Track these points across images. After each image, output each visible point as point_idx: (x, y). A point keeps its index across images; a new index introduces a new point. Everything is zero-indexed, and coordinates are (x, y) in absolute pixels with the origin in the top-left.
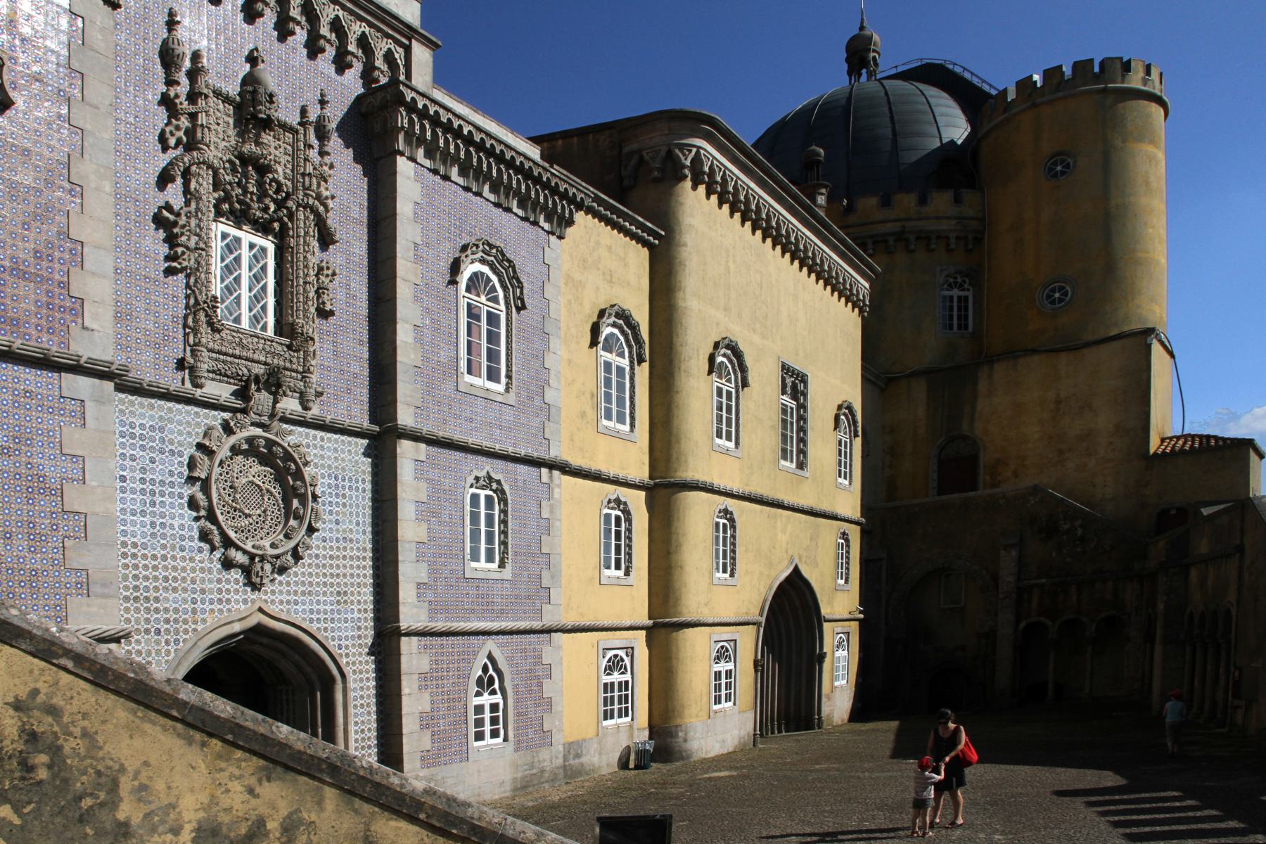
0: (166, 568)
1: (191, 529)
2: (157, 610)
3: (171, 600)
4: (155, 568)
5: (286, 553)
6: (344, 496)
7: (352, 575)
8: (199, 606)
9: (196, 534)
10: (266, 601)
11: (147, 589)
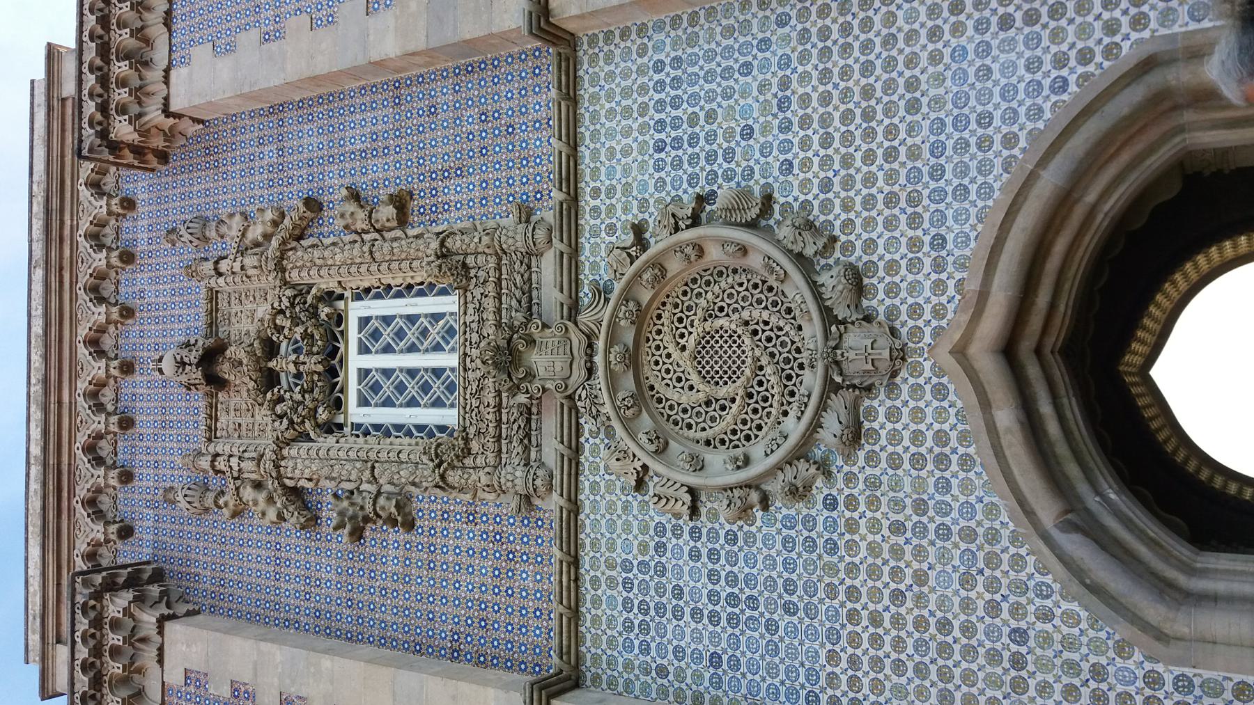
0: (875, 594)
1: (790, 523)
2: (968, 630)
3: (944, 590)
4: (876, 620)
10: (937, 332)
11: (921, 645)
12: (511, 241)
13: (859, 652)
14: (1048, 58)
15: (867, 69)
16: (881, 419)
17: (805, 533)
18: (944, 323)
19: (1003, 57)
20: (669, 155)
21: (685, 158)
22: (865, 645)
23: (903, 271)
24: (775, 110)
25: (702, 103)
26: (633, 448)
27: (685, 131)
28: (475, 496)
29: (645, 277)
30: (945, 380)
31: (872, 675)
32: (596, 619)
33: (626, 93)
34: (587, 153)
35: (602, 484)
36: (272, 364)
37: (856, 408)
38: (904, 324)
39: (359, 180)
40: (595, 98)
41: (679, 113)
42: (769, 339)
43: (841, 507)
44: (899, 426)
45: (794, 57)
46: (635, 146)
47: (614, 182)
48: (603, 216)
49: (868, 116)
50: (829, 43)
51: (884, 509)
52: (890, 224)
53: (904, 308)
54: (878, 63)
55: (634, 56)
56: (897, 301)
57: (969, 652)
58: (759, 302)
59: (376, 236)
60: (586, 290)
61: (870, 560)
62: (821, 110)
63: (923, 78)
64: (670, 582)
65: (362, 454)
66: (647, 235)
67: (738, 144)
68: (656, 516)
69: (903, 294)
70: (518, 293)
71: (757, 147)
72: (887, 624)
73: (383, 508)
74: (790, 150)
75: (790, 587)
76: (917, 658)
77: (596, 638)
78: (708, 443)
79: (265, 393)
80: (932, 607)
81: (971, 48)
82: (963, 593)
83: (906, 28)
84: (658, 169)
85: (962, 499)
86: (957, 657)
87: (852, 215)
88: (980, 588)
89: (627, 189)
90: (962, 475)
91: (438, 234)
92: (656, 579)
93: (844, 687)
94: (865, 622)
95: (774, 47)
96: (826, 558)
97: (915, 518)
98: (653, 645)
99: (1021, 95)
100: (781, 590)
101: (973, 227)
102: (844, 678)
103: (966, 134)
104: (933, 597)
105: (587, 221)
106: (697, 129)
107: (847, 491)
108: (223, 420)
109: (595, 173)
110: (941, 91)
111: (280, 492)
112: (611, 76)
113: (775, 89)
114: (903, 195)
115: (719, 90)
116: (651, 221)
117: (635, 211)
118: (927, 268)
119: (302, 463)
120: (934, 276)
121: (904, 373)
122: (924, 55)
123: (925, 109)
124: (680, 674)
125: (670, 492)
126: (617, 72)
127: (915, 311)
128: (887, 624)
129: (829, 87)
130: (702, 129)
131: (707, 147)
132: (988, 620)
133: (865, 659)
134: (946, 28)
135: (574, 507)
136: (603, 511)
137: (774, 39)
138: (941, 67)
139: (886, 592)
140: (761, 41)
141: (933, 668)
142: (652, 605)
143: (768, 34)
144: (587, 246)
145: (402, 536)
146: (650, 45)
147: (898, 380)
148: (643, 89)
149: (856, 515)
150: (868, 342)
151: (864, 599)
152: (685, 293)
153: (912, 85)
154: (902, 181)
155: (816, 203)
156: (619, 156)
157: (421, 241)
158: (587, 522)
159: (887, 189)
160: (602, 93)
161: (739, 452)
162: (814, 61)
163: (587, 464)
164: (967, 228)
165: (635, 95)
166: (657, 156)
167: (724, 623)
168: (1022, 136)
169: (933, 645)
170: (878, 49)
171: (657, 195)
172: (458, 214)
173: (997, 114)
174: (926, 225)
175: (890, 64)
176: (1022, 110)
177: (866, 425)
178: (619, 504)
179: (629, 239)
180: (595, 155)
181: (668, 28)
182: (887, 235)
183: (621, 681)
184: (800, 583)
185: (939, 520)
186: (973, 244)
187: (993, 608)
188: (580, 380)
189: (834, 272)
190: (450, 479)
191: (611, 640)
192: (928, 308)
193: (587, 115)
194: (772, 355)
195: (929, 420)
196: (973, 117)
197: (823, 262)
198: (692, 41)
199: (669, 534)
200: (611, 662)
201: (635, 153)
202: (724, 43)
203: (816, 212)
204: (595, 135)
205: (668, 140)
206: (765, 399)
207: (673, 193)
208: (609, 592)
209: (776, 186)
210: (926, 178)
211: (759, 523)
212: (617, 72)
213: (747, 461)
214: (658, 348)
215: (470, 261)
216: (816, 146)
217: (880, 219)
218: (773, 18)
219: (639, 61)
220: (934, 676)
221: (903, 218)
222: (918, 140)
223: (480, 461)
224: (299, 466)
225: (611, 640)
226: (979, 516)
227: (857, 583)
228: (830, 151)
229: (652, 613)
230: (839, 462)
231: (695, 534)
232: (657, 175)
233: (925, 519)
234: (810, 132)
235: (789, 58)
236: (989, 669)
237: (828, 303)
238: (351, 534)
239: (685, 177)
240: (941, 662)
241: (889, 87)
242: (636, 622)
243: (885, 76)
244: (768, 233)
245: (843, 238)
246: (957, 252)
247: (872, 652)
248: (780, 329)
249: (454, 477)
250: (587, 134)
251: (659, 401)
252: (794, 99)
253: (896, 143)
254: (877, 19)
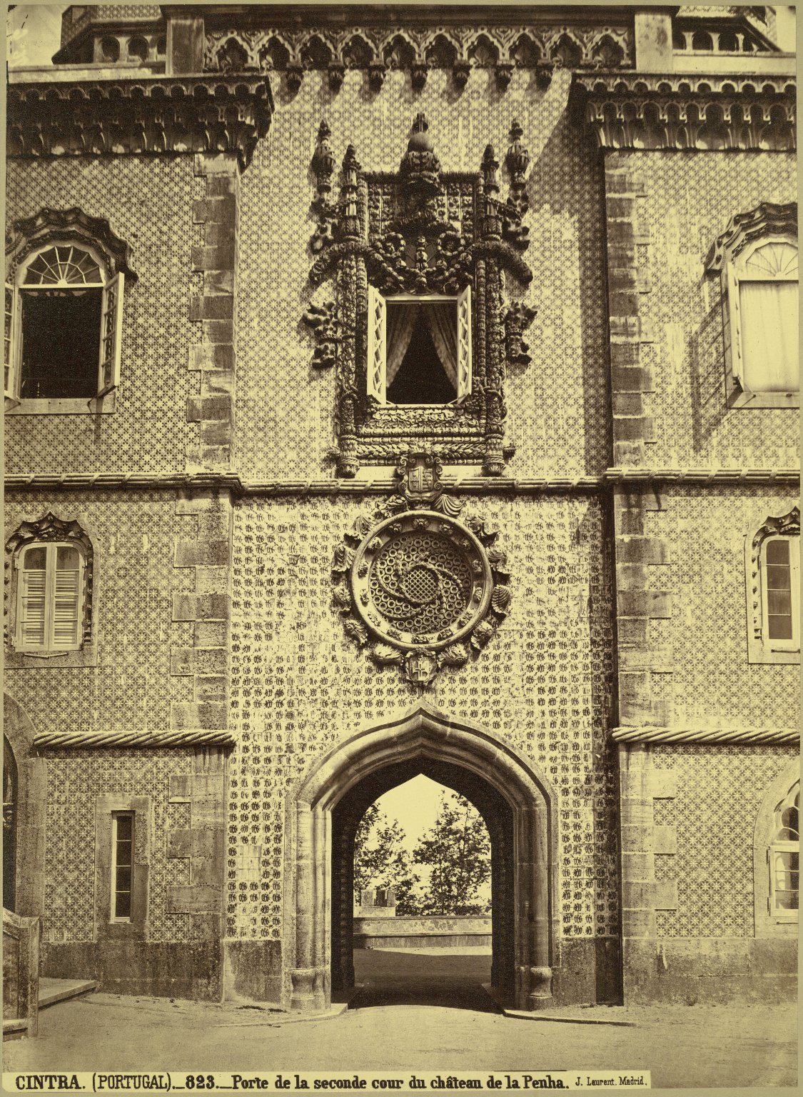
5: (455, 642)
26: (370, 534)
73: (326, 347)
78: (374, 575)
161: (369, 595)
179: (489, 531)
213: (365, 604)
244: (483, 617)
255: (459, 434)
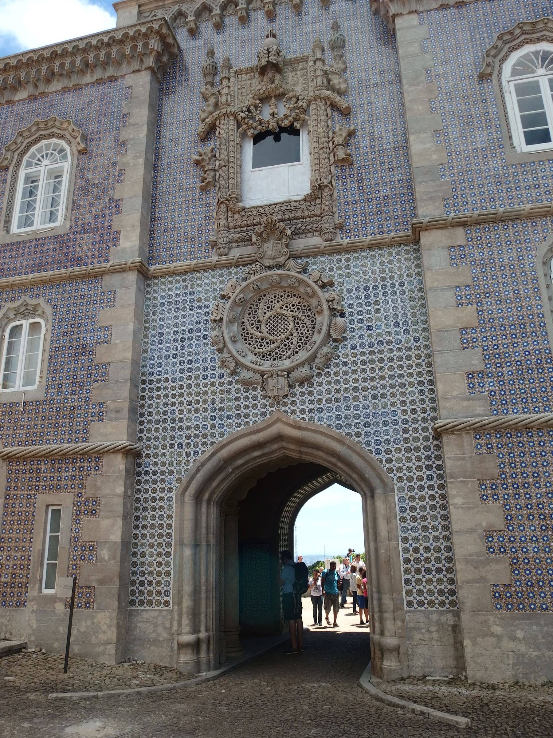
0: (190, 394)
2: (181, 429)
3: (193, 419)
4: (181, 395)
5: (301, 364)
6: (377, 303)
7: (392, 377)
8: (217, 422)
9: (218, 364)
10: (286, 412)
12: (326, 221)
13: (169, 390)
14: (390, 447)
15: (392, 377)
16: (253, 393)
17: (209, 367)
18: (289, 414)
19: (391, 430)
20: (362, 293)
21: (361, 301)
22: (172, 392)
23: (310, 398)
24: (378, 340)
25: (384, 306)
27: (372, 299)
28: (216, 219)
29: (309, 289)
30: (268, 416)
31: (162, 395)
32: (171, 282)
33: (391, 270)
34: (366, 254)
35: (223, 278)
36: (273, 99)
37: (256, 383)
38: (289, 399)
39: (359, 133)
40: (390, 254)
41: (381, 296)
42: (285, 345)
43: (220, 380)
44: (250, 400)
45: (400, 346)
46: (367, 277)
47: (352, 268)
48: (337, 265)
49: (373, 379)
50: (404, 360)
51: (220, 396)
52: (328, 391)
53: (295, 399)
54: (394, 381)
55: (408, 272)
56: (298, 396)
57: (173, 429)
58: (301, 340)
59: (331, 148)
60: (305, 260)
61: (201, 392)
62: (376, 359)
63: (386, 400)
64: (187, 313)
65: (231, 159)
66: (328, 287)
67: (365, 325)
68: (212, 304)
69: (300, 398)
70: (303, 228)
71: (363, 333)
72: (180, 399)
74: (361, 348)
75: (190, 362)
76: (169, 411)
77: (163, 283)
78: (243, 323)
79: (260, 99)
80: (187, 415)
81: (396, 418)
82: (193, 426)
83: (407, 392)
84: (356, 289)
85: (225, 424)
86: (171, 425)
87: (332, 376)
88: (195, 432)
89: (349, 275)
90: (234, 424)
91: (331, 182)
92: (188, 307)
93: (157, 385)
94: (180, 391)
95: (405, 336)
96: (201, 376)
97: (217, 408)
98: (163, 308)
99: (376, 438)
100: (188, 358)
101: (325, 423)
102: (160, 385)
103: (362, 418)
104: (190, 415)
105: (335, 258)
106: (373, 305)
107: (225, 382)
108: (245, 77)
109: (356, 259)
110: (380, 407)
111: (214, 119)
112: (399, 261)
113: (387, 338)
114: (339, 396)
115: (389, 314)
116: (334, 288)
117: (339, 280)
118: (310, 407)
119: (227, 128)
120: (307, 409)
121: (270, 401)
122: (395, 400)
123: (373, 401)
124: (154, 320)
125: (220, 310)
126: (401, 264)
127: (294, 403)
128: (180, 399)
129: (386, 362)
130: (373, 308)
131: (364, 311)
132: (184, 435)
133: (167, 392)
134: (406, 408)
135: (214, 267)
136: (213, 280)
137: (409, 336)
138: (389, 406)
139: (191, 399)
140: (408, 330)
141: (166, 417)
142: (178, 306)
143: (411, 333)
144: (324, 259)
145: (199, 184)
146: (412, 279)
147: (268, 398)
148: (392, 278)
149: (217, 386)
150: (280, 387)
151: (188, 391)
152: (305, 306)
153: (384, 396)
154: (345, 395)
155: (338, 361)
156: (363, 269)
157: (327, 174)
158: (208, 274)
159: (342, 389)
160: (392, 258)
162: (398, 354)
163: (231, 270)
164: (325, 420)
165: (390, 274)
166: (362, 288)
167: (175, 337)
168: (360, 439)
169: (174, 416)
170: (399, 381)
171: (345, 290)
172: (341, 191)
173: (369, 429)
174: (327, 405)
175: (393, 386)
176: (370, 439)
177: (250, 388)
178: (216, 287)
179: (325, 280)
180: (365, 258)
181: (419, 287)
182: (324, 390)
183: (150, 296)
184: (191, 366)
185: (217, 416)
186: (319, 423)
187: (189, 437)
188: (264, 264)
189: (308, 371)
190: (222, 206)
191: (163, 290)
192: (295, 408)
193: (383, 252)
194: (279, 347)
195: (253, 411)
196: (368, 420)
197: (314, 366)
198: (412, 299)
199: (205, 310)
200: (156, 291)
201: (364, 277)
202: (409, 314)
203: (335, 361)
204: (373, 257)
205: (369, 292)
206: (261, 346)
207: (346, 297)
208: (182, 287)
209: (346, 343)
210: (345, 404)
211: (212, 348)
212: (401, 264)
214: (282, 296)
215: (318, 201)
216: (362, 358)
217: (330, 387)
218: (418, 335)
219: (405, 274)
220: (164, 417)
221: (330, 396)
222: (361, 400)
223: (230, 219)
224: (225, 127)
225: (163, 290)
226: (220, 430)
227: (193, 387)
228: (359, 365)
229: (176, 306)
230: (236, 378)
231: (206, 322)
232: (354, 289)
233: (217, 411)
234: (368, 355)
235: (400, 343)
236: (168, 436)
237: (296, 370)
238: (197, 160)
239: (352, 302)
240: (169, 419)
241: (384, 387)
242: (171, 300)
243: (388, 385)
244: (324, 343)
245: (323, 373)
246: (316, 417)
247: (170, 395)
248: (289, 349)
249: (223, 208)
250: (374, 253)
251: (259, 300)
252: (382, 347)
253: (360, 391)
254: (412, 379)
255: (302, 218)
